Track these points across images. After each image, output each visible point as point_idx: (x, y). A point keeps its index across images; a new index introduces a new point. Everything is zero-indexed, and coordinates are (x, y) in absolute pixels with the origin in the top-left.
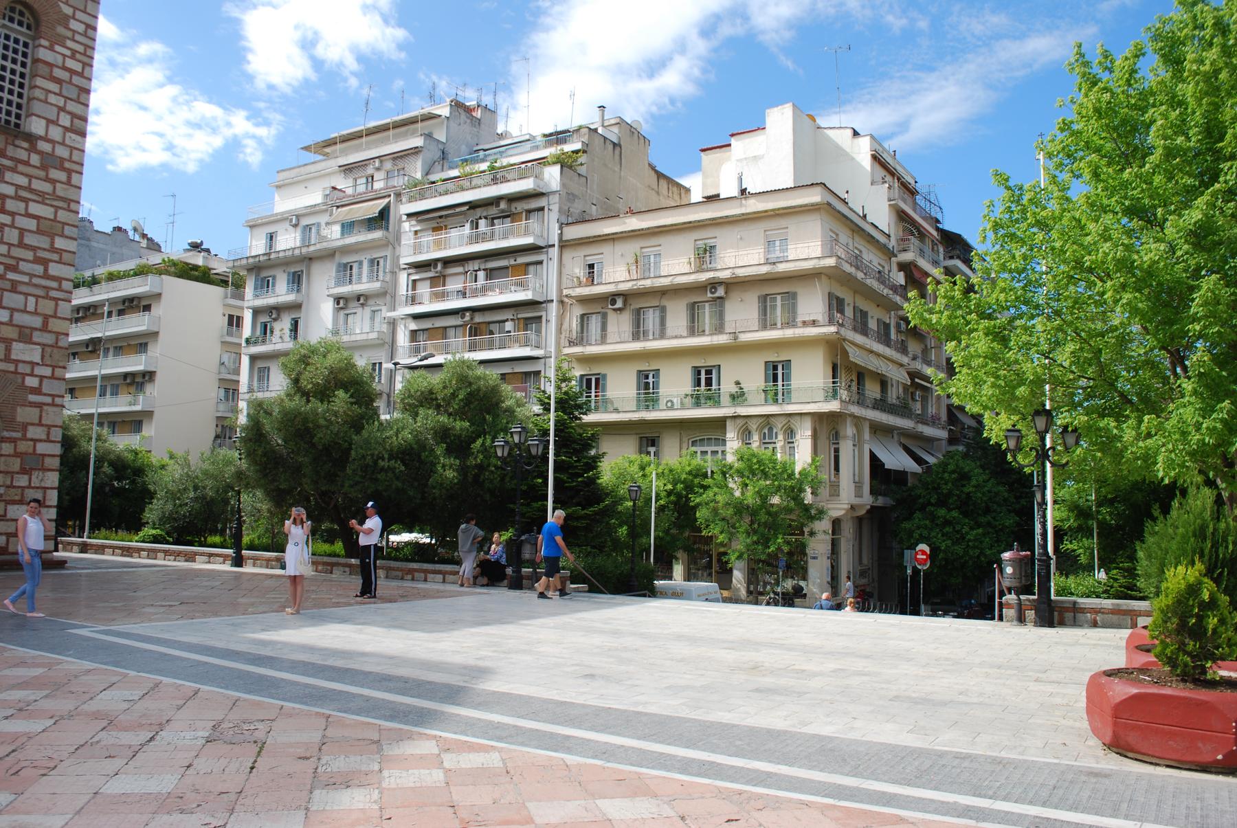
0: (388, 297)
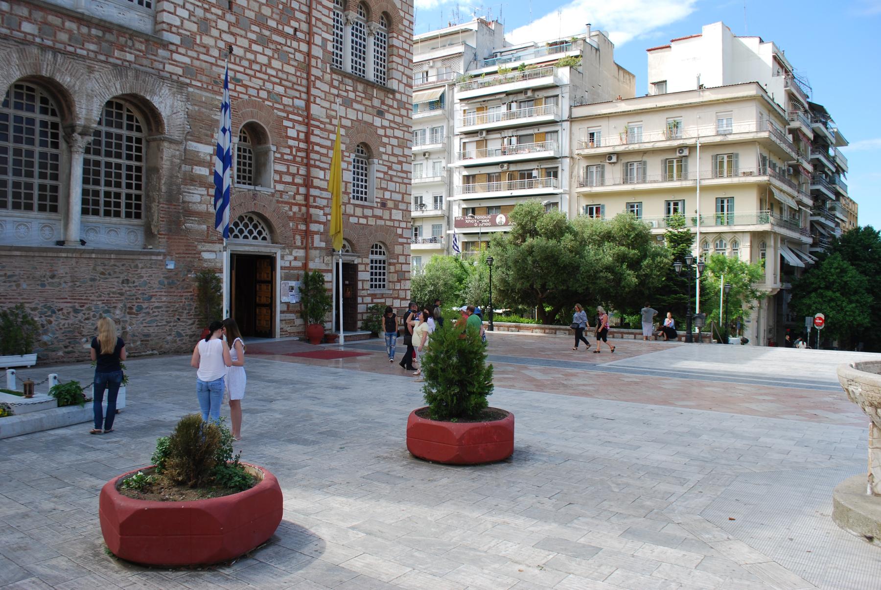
0: (446, 153)
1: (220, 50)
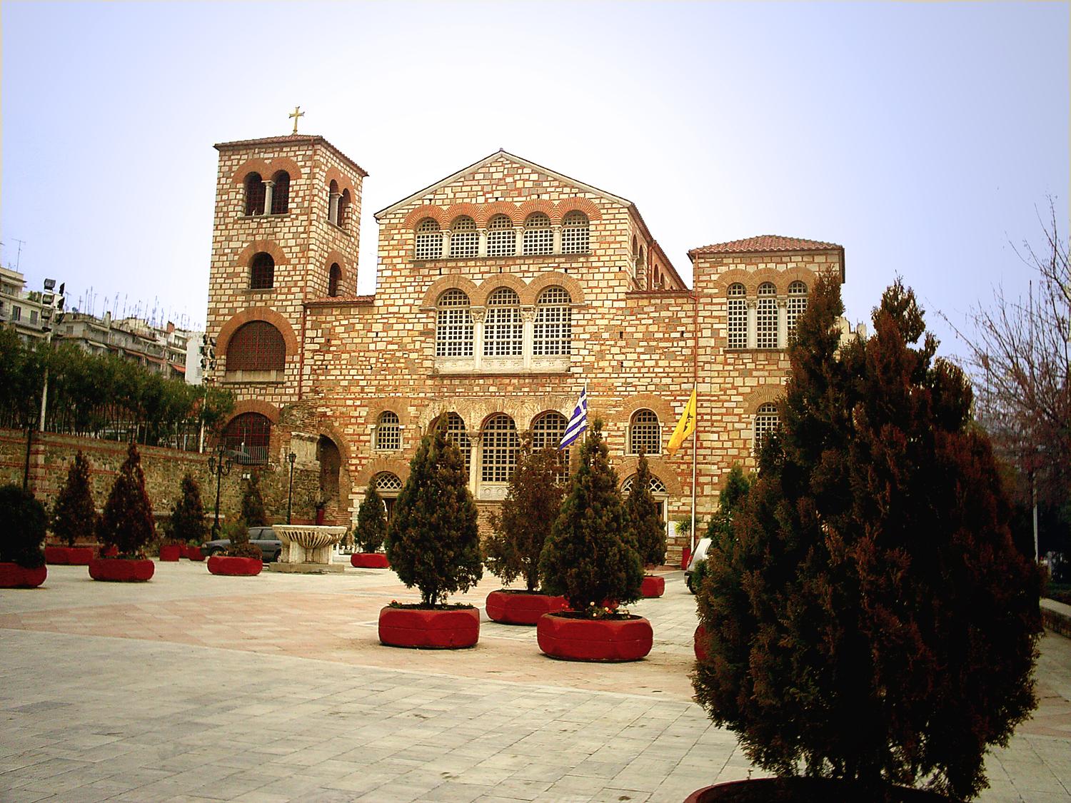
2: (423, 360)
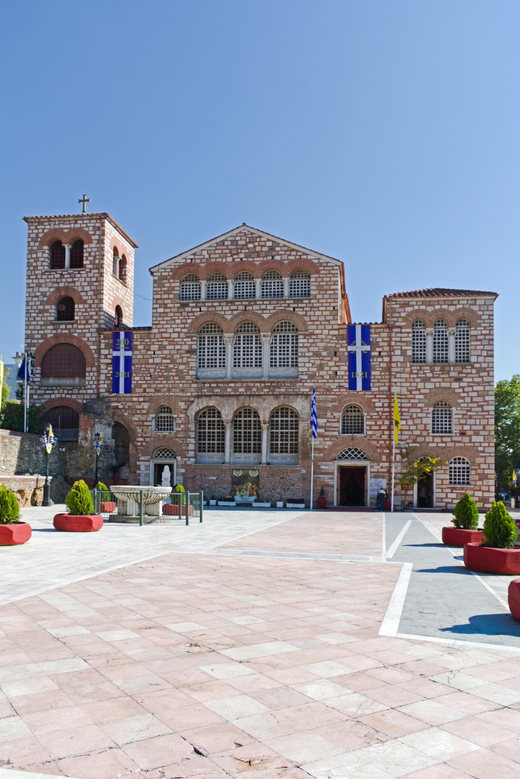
1: (330, 375)
2: (189, 370)
